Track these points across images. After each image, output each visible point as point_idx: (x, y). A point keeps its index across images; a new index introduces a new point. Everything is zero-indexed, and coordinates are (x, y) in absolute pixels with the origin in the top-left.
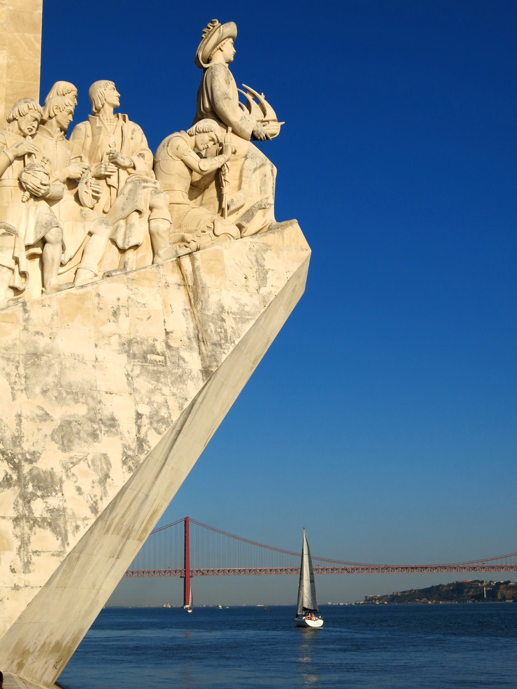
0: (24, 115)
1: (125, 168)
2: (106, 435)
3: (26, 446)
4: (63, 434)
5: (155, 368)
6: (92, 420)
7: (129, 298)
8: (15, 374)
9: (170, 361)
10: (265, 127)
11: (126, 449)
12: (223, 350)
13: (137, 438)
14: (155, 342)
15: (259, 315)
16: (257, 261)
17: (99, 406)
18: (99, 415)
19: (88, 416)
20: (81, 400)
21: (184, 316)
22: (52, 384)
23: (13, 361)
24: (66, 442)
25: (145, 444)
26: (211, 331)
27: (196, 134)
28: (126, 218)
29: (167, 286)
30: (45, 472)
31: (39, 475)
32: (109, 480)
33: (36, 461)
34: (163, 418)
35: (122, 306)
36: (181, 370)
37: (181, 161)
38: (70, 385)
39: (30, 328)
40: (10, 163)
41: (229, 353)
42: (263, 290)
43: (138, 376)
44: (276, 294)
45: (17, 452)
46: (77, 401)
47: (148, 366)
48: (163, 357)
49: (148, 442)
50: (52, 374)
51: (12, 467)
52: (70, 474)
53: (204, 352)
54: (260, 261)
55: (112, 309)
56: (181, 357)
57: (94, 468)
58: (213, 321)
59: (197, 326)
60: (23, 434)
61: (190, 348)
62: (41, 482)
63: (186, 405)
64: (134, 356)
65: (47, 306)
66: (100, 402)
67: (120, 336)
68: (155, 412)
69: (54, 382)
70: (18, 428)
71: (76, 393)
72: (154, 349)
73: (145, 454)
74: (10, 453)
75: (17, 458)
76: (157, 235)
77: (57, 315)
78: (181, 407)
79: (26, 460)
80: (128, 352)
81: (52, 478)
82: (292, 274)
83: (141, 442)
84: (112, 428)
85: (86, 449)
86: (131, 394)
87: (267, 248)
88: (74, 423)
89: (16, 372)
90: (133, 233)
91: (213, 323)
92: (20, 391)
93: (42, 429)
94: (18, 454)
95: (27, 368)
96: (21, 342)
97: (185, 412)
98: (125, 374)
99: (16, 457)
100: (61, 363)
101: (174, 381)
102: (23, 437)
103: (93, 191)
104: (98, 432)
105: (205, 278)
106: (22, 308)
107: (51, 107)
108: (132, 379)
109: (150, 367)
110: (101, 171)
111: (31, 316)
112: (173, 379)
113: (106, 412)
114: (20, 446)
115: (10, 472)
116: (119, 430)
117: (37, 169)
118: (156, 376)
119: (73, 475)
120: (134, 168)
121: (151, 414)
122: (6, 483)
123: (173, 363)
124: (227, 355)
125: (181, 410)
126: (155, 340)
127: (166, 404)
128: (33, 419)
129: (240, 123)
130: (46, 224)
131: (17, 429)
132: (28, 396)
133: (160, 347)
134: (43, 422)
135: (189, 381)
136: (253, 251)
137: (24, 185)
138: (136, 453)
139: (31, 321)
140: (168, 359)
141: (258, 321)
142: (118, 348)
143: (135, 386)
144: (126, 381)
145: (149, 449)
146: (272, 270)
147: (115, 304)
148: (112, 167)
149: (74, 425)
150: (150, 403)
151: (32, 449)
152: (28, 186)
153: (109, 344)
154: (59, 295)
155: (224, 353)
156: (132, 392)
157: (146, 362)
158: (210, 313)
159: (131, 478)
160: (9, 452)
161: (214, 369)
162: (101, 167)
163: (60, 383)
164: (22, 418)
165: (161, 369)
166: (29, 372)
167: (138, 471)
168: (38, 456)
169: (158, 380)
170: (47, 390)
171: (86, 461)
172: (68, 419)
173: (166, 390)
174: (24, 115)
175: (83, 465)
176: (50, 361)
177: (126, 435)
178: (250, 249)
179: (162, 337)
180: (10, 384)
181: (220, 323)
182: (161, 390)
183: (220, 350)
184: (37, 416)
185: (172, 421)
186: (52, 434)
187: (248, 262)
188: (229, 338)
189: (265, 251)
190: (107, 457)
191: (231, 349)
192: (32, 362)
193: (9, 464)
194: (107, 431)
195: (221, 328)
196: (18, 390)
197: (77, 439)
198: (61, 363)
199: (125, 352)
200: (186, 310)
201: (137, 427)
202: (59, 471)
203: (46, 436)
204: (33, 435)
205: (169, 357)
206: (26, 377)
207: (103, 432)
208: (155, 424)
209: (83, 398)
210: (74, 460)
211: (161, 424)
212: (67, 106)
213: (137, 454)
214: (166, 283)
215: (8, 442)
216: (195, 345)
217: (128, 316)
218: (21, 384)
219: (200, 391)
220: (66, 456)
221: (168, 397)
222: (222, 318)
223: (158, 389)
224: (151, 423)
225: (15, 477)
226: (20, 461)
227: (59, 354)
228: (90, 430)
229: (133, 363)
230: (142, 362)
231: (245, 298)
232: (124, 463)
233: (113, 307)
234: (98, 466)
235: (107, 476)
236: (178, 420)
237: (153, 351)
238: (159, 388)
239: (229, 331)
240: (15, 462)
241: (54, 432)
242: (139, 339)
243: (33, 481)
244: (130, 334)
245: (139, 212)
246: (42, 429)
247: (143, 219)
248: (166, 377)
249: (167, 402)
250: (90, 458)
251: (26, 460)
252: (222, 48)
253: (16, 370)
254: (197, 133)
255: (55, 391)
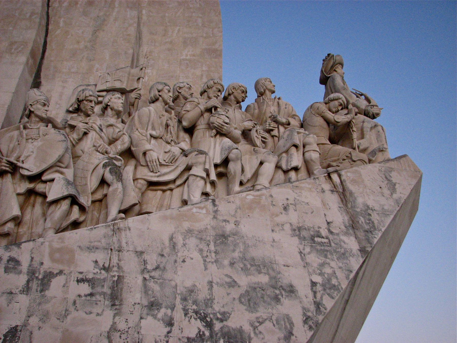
0: (211, 88)
1: (283, 124)
2: (287, 299)
3: (217, 307)
4: (249, 297)
5: (322, 248)
6: (274, 287)
7: (295, 198)
8: (206, 250)
9: (333, 242)
10: (372, 109)
11: (306, 311)
12: (374, 236)
13: (314, 302)
14: (320, 229)
15: (396, 212)
16: (386, 178)
17: (279, 276)
18: (280, 283)
19: (270, 283)
20: (263, 271)
21: (340, 212)
22: (238, 258)
23: (205, 240)
24: (252, 304)
25: (321, 306)
26: (362, 222)
27: (329, 103)
28: (287, 152)
29: (323, 191)
30: (234, 330)
31: (229, 332)
32: (293, 338)
33: (226, 320)
34: (334, 286)
35: (291, 204)
36: (343, 250)
37: (322, 118)
38: (253, 259)
39: (218, 217)
40: (202, 115)
41: (379, 237)
42: (395, 196)
43: (309, 253)
44: (405, 198)
45: (209, 312)
46: (260, 272)
47: (316, 246)
48: (328, 240)
49: (324, 305)
50: (238, 250)
51: (205, 324)
52: (257, 331)
53: (359, 236)
54: (388, 177)
55: (283, 206)
56: (341, 240)
57: (279, 327)
58: (363, 215)
59: (350, 218)
60: (214, 297)
61: (346, 234)
62: (231, 338)
63: (352, 276)
64: (304, 239)
65: (231, 202)
66: (279, 273)
67: (291, 224)
68: (327, 281)
69: (240, 257)
70: (210, 292)
71: (259, 266)
72: (319, 234)
73: (323, 315)
74: (203, 312)
75: (209, 317)
76: (311, 162)
77: (240, 209)
78: (347, 278)
79: (218, 319)
80: (299, 236)
81: (241, 335)
82: (413, 186)
83: (318, 305)
84: (291, 294)
85: (270, 310)
86: (304, 267)
87: (391, 170)
88: (258, 289)
89: (208, 248)
90: (293, 159)
91: (362, 217)
92: (211, 263)
93: (230, 293)
94: (209, 314)
95: (217, 246)
96: (212, 227)
97: (351, 281)
98: (299, 252)
99: (208, 316)
100: (244, 243)
101: (339, 257)
102: (214, 299)
103: (262, 137)
104: (280, 297)
105: (350, 186)
106: (212, 203)
107: (230, 87)
108: (304, 255)
109: (318, 247)
110: (267, 126)
111: (219, 209)
112: (338, 256)
113: (285, 281)
114: (211, 307)
115: (203, 329)
116: (298, 295)
117: (220, 113)
118: (324, 253)
119: (260, 332)
120: (289, 124)
121: (324, 282)
122: (199, 339)
123: (336, 244)
124: (378, 239)
125: (348, 279)
126: (319, 227)
127: (334, 275)
128: (222, 285)
129: (356, 102)
130: (228, 147)
131: (209, 293)
132: (218, 267)
133: (324, 232)
134: (231, 288)
135: (351, 257)
136: (382, 171)
137: (211, 125)
138: (315, 314)
139: (219, 213)
140: (331, 242)
141: (395, 216)
142: (291, 233)
143: (307, 261)
144: (300, 257)
145: (325, 311)
146: (399, 184)
147: (285, 202)
148: (273, 124)
149: (258, 291)
150: (321, 274)
151: (222, 310)
152: (214, 124)
153: (283, 229)
154: (240, 196)
155: (375, 237)
156: (306, 264)
157: (314, 243)
158: (358, 210)
159: (312, 336)
160: (201, 311)
161: (369, 249)
162: (266, 124)
163: (245, 257)
164: (213, 284)
165: (327, 248)
166: (218, 248)
167: (318, 330)
168: (228, 316)
169: (326, 256)
170: (234, 263)
171: (271, 321)
172: (253, 285)
173: (333, 264)
174: (211, 88)
175: (268, 324)
176: (235, 241)
177: (305, 300)
178: (379, 170)
179: (325, 226)
180: (203, 257)
181: (367, 217)
182: (329, 264)
183: (372, 235)
184: (226, 282)
185: (342, 288)
186: (240, 298)
187: (380, 178)
188: (376, 227)
189: (391, 172)
190: (289, 317)
191: (380, 234)
192: (220, 242)
193: (202, 322)
194: (287, 296)
195: (369, 220)
196: (209, 262)
197: (262, 302)
198: (244, 243)
199: (296, 236)
200: (340, 207)
201: (313, 293)
202: (247, 328)
203: (234, 299)
204: (223, 299)
205: (332, 240)
206: (215, 252)
207: (284, 296)
208: (328, 291)
209: (265, 270)
210: (261, 320)
211: (333, 291)
212: (240, 87)
213: (315, 315)
214: (322, 189)
215: (201, 304)
216: (351, 231)
217: (296, 211)
218: (212, 257)
219: (361, 265)
220: (253, 316)
221: (336, 270)
222: (369, 213)
223: (327, 263)
224: (325, 290)
225: (207, 333)
226: (211, 320)
227: (243, 236)
228: (273, 295)
229: (304, 244)
230: (311, 243)
231: (383, 201)
232: (305, 322)
233: (283, 204)
234: (282, 326)
235: (291, 334)
236: (346, 288)
237: (320, 236)
238: (327, 262)
239: (376, 222)
240: (207, 321)
241: (241, 296)
242: (306, 227)
243: (224, 338)
244: (299, 223)
245: (296, 146)
246: (230, 293)
247: (299, 152)
248: (331, 254)
249: (335, 274)
250: (274, 318)
251: (218, 319)
252: (337, 70)
253: (207, 247)
254: (329, 102)
255: (241, 264)
